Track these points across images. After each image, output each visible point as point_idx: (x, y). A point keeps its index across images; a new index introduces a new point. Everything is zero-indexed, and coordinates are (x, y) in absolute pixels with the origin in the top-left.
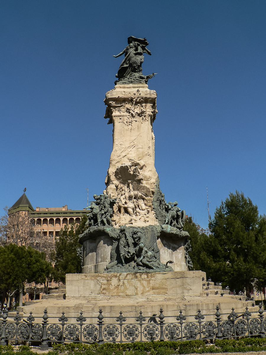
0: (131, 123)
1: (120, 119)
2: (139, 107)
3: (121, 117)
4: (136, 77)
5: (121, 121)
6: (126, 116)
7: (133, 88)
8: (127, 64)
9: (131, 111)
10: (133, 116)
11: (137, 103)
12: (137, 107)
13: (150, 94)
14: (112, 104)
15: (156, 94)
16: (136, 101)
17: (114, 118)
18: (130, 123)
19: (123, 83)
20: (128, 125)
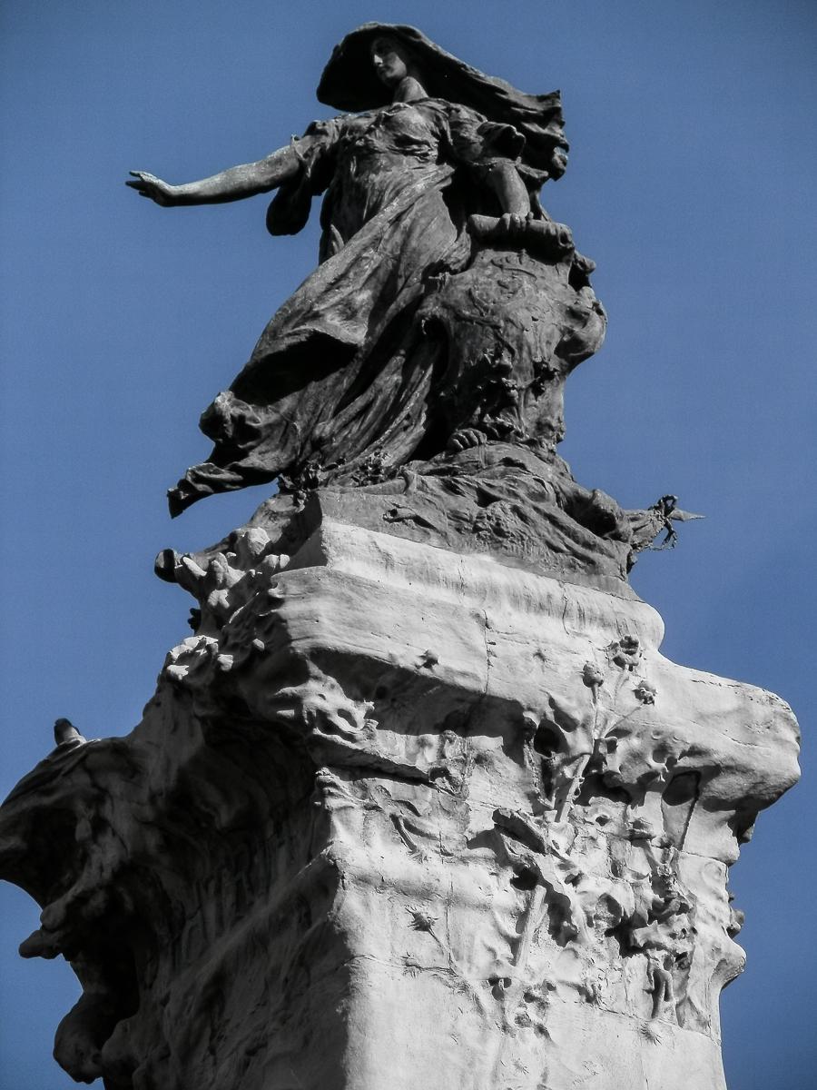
0: (543, 1005)
1: (422, 925)
2: (602, 841)
3: (427, 911)
4: (541, 497)
5: (423, 948)
6: (485, 907)
7: (515, 600)
8: (349, 312)
9: (548, 867)
10: (562, 932)
11: (601, 783)
12: (592, 831)
13: (747, 727)
14: (331, 728)
15: (790, 736)
16: (597, 760)
17: (351, 901)
18: (529, 997)
19: (399, 520)
20: (511, 1021)
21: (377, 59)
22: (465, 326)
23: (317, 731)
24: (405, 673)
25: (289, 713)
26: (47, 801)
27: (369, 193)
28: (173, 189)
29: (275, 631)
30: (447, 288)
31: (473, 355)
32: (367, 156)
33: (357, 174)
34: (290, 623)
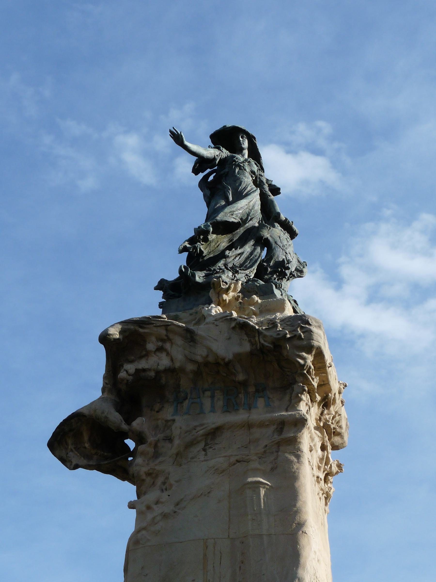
21: (241, 139)
22: (277, 247)
23: (305, 372)
24: (325, 366)
25: (302, 362)
26: (141, 330)
27: (243, 183)
28: (186, 143)
29: (307, 333)
30: (271, 231)
31: (278, 257)
32: (242, 169)
33: (238, 173)
34: (315, 334)
